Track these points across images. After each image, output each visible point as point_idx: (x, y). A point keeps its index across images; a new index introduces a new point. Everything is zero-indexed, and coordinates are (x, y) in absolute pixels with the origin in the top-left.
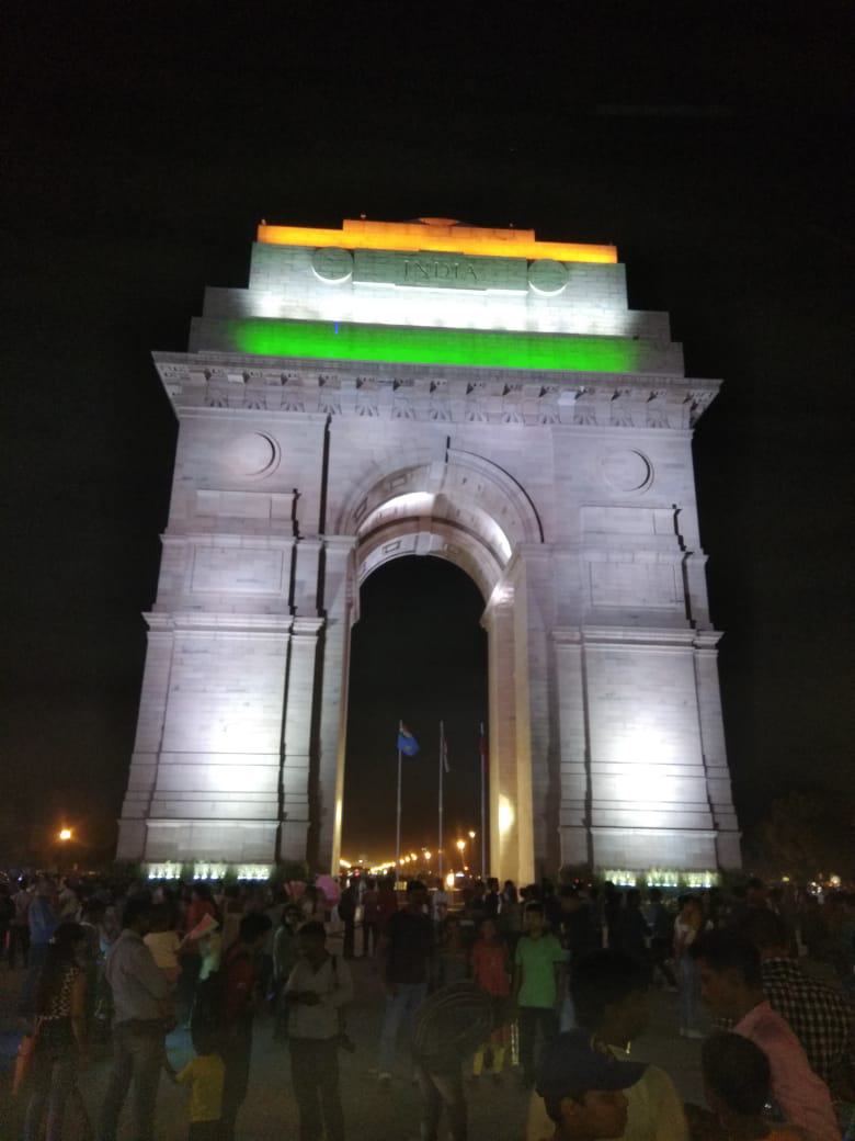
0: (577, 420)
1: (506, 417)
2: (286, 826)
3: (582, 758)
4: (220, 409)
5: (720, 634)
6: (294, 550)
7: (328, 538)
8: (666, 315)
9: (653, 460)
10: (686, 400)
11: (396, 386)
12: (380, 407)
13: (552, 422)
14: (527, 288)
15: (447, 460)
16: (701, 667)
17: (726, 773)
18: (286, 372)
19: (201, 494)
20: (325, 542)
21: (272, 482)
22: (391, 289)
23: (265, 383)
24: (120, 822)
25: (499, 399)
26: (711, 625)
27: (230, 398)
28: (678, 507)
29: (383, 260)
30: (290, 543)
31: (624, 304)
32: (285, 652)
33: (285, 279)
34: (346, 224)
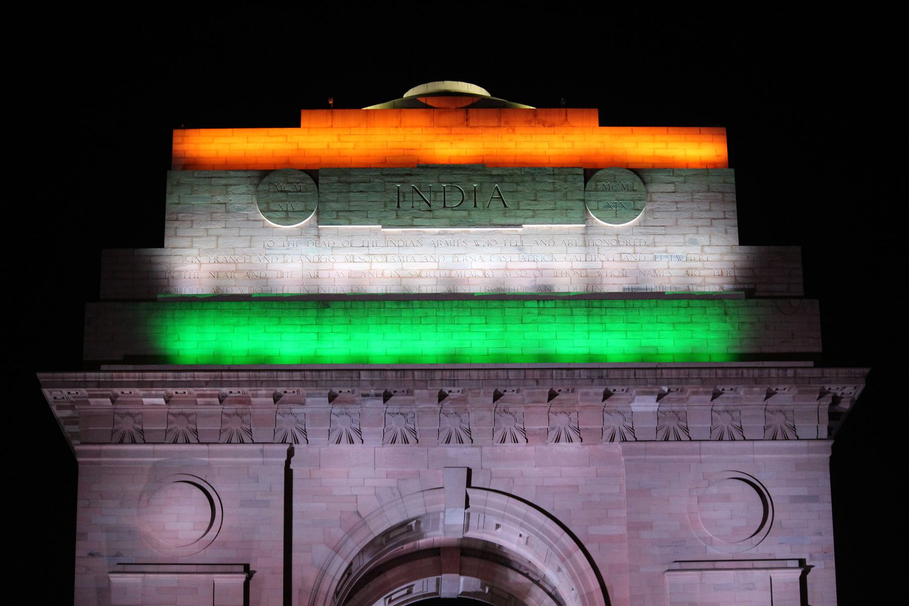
1: (553, 435)
9: (775, 491)
10: (823, 394)
11: (387, 397)
12: (364, 429)
13: (624, 440)
14: (585, 219)
15: (467, 506)
19: (116, 579)
21: (212, 555)
22: (376, 233)
23: (196, 403)
25: (543, 408)
28: (808, 563)
29: (362, 187)
31: (734, 239)
33: (216, 228)
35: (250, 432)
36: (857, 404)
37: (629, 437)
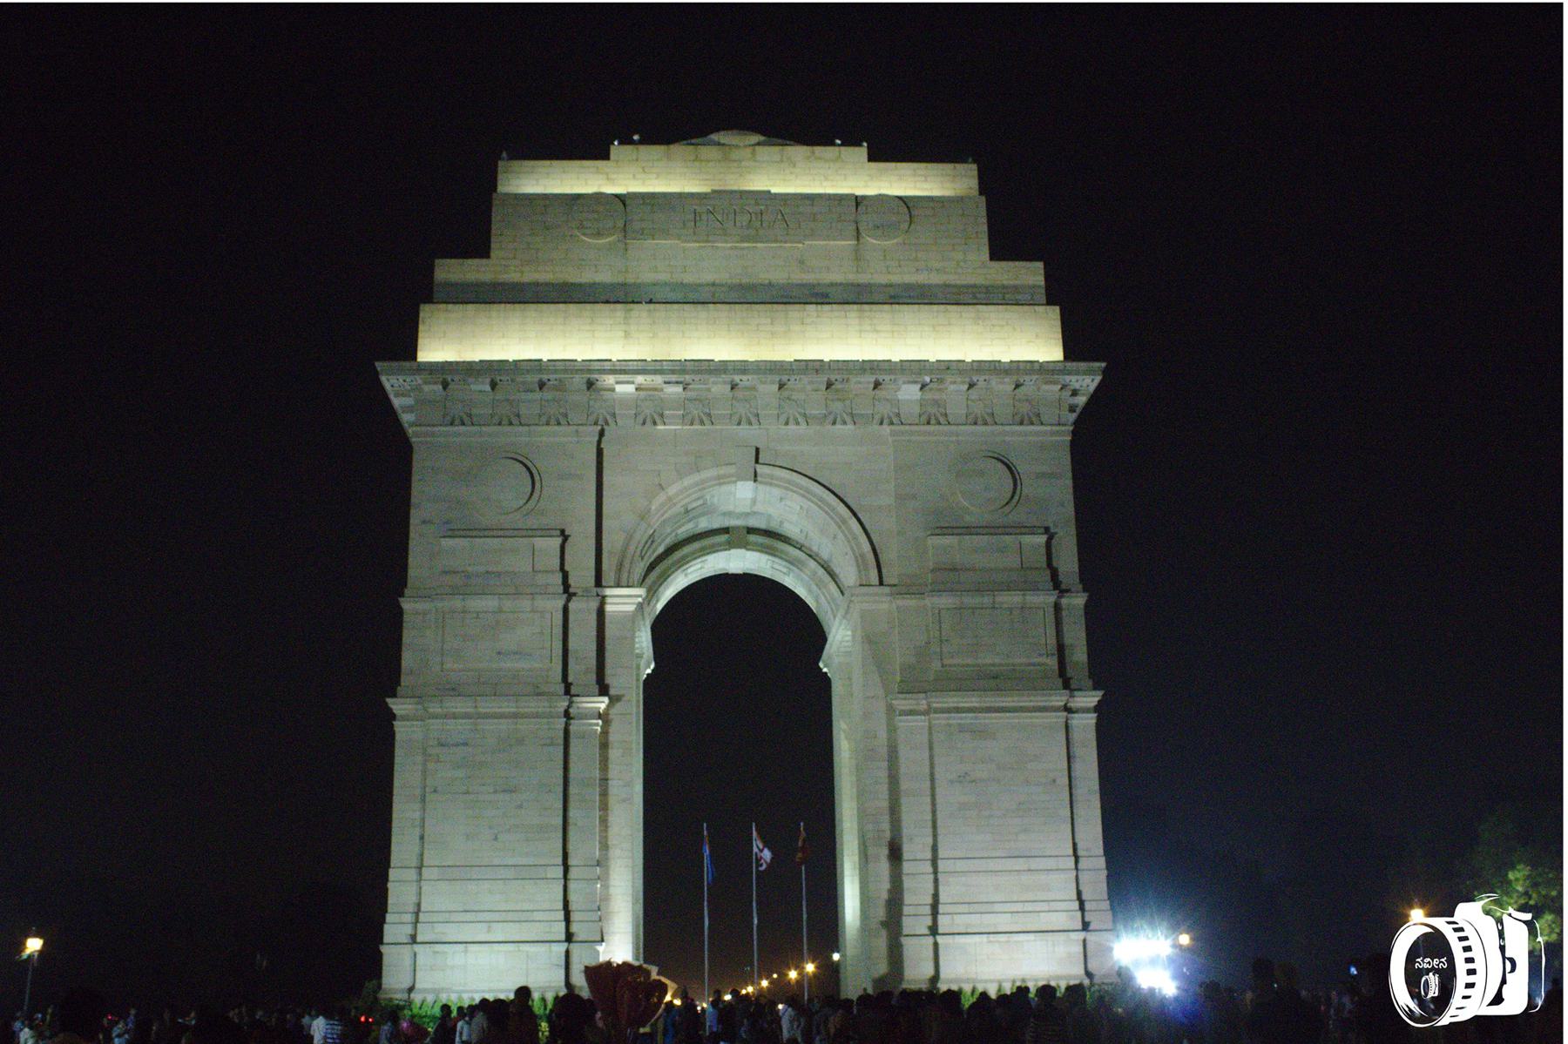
0: (924, 419)
2: (575, 948)
3: (929, 855)
4: (463, 428)
5: (1100, 693)
6: (566, 610)
7: (608, 592)
8: (1040, 265)
9: (1021, 468)
13: (892, 423)
14: (858, 237)
16: (1076, 736)
17: (1102, 862)
18: (545, 377)
19: (444, 542)
20: (604, 597)
21: (533, 522)
24: (384, 949)
26: (1091, 683)
27: (474, 411)
30: (560, 603)
32: (561, 741)
34: (616, 149)
35: (566, 416)
36: (1095, 398)
37: (895, 420)
